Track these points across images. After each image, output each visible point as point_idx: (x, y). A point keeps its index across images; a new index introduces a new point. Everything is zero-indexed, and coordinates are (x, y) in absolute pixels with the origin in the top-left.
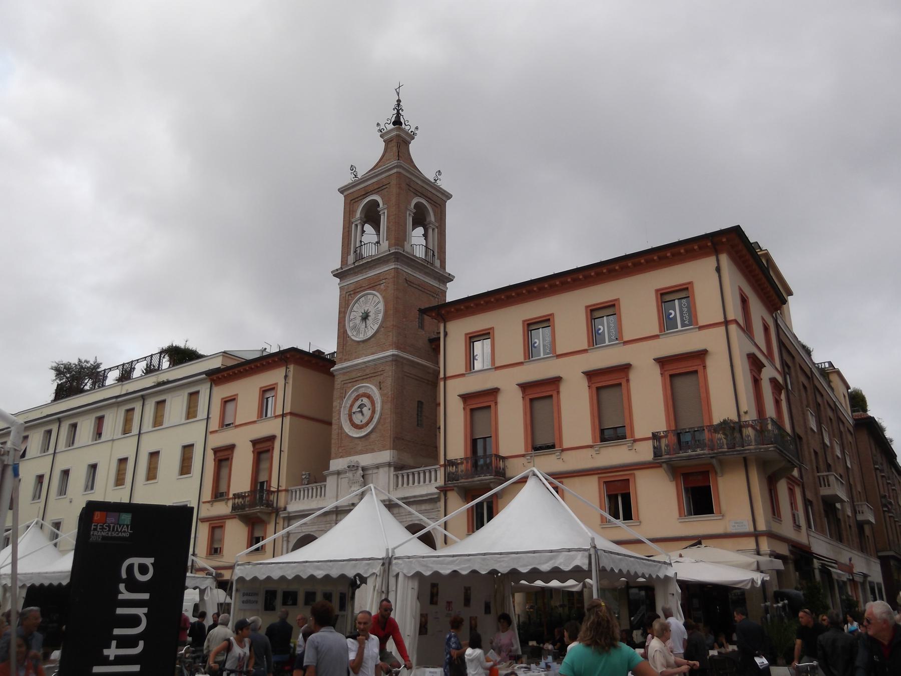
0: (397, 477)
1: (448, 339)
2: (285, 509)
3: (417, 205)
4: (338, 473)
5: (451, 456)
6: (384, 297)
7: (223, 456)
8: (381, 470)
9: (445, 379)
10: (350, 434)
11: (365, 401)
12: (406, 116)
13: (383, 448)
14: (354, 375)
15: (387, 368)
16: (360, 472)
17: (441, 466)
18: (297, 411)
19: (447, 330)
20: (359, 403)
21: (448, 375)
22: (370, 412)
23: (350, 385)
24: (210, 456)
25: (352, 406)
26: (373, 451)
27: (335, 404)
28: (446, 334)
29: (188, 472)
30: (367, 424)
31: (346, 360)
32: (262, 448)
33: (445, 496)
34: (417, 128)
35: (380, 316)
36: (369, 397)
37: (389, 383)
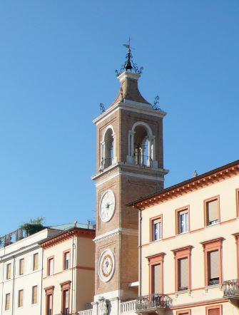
1: (142, 221)
3: (138, 129)
4: (97, 303)
5: (143, 295)
7: (49, 292)
9: (141, 247)
11: (108, 260)
12: (134, 61)
16: (105, 303)
18: (81, 265)
19: (142, 216)
20: (106, 261)
21: (143, 244)
24: (44, 291)
27: (96, 261)
29: (36, 302)
32: (65, 287)
34: (142, 68)
37: (118, 248)
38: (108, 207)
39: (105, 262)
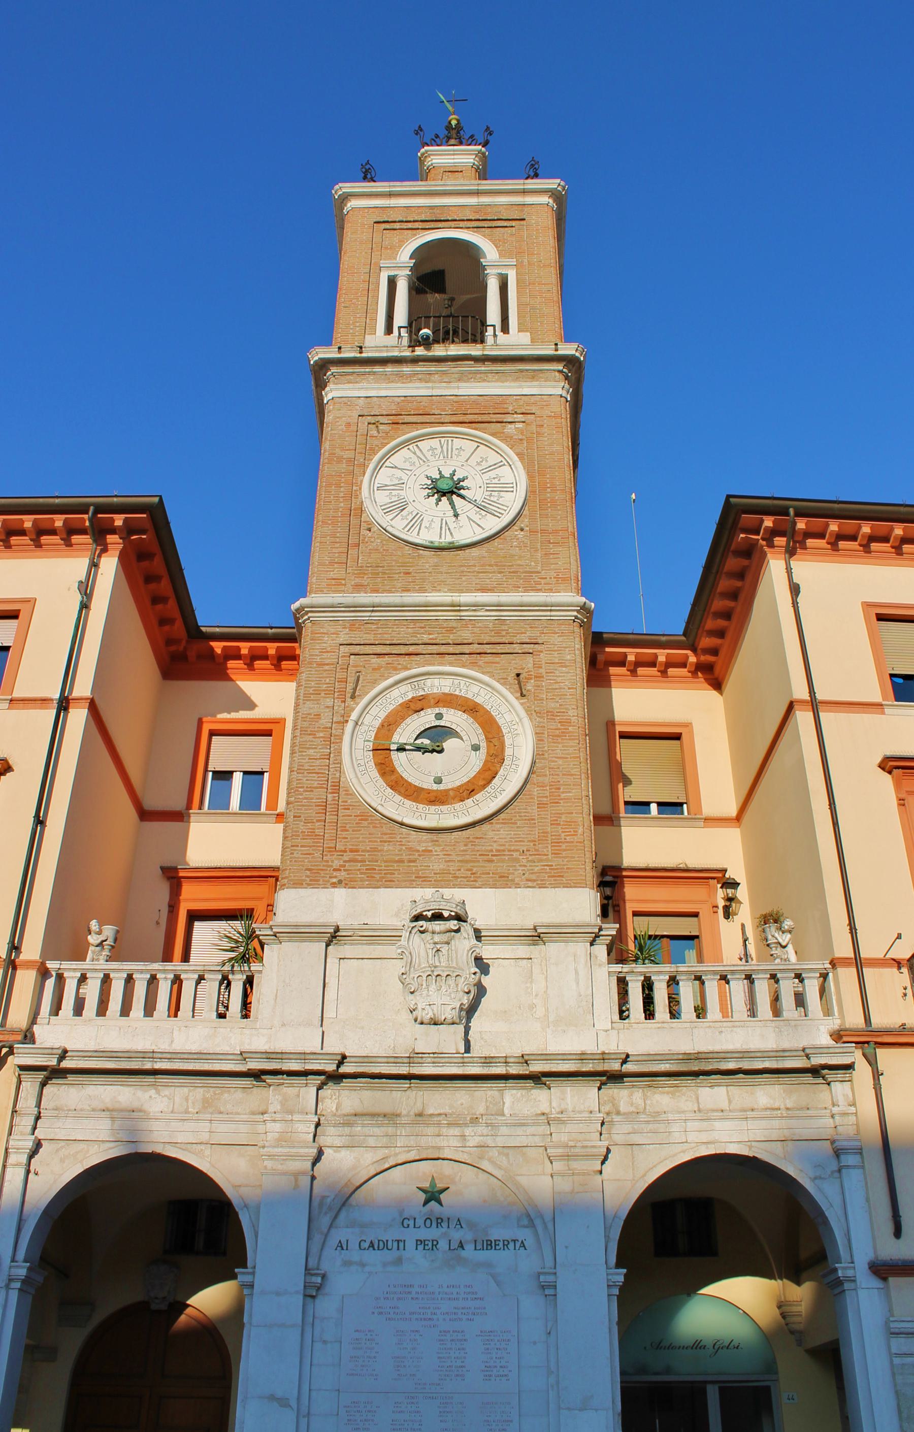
0: (622, 983)
2: (28, 1037)
6: (520, 455)
8: (552, 949)
10: (391, 810)
11: (453, 718)
13: (557, 878)
14: (403, 634)
15: (556, 639)
17: (845, 962)
20: (427, 719)
21: (819, 697)
22: (476, 761)
23: (375, 660)
25: (390, 724)
26: (503, 881)
28: (795, 590)
30: (469, 791)
31: (358, 588)
33: (872, 1061)
35: (513, 502)
36: (472, 709)
38: (447, 490)
39: (427, 719)
